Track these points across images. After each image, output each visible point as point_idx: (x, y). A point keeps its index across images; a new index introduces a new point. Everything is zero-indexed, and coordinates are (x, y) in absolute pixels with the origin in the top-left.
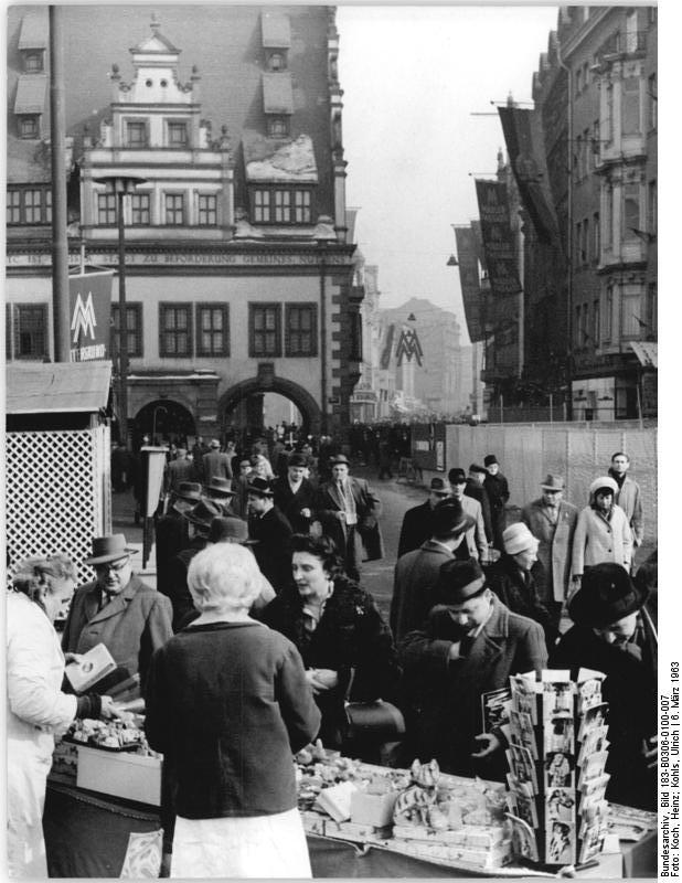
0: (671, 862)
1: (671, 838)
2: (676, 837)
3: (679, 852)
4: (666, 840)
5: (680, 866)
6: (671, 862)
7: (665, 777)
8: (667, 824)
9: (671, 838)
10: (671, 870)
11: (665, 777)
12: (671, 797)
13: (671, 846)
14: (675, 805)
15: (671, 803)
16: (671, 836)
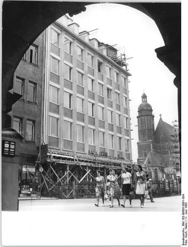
1: (185, 235)
2: (186, 234)
3: (187, 238)
4: (184, 235)
5: (187, 242)
8: (184, 230)
9: (185, 235)
11: (183, 217)
14: (186, 225)
15: (185, 225)
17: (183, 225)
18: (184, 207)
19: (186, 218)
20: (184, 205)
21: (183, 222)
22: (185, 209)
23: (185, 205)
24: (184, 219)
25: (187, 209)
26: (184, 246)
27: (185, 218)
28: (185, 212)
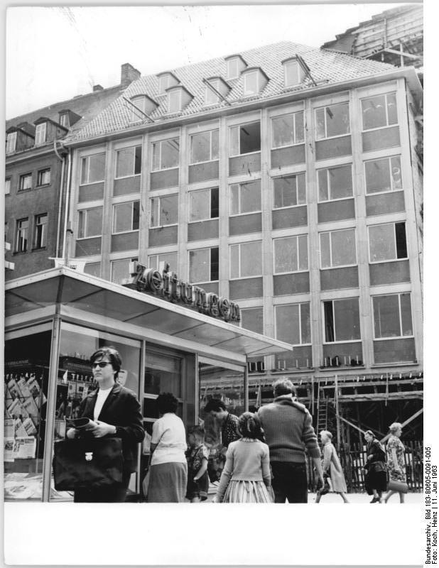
0: (432, 554)
1: (432, 541)
2: (435, 539)
3: (437, 548)
4: (429, 540)
5: (438, 557)
6: (432, 554)
7: (428, 500)
8: (429, 530)
9: (432, 539)
10: (432, 559)
11: (428, 500)
12: (432, 513)
13: (432, 544)
14: (435, 518)
15: (432, 517)
16: (432, 538)
17: (428, 518)
18: (431, 475)
19: (434, 501)
20: (431, 470)
21: (429, 511)
22: (432, 480)
23: (432, 472)
24: (431, 504)
25: (437, 480)
26: (431, 565)
27: (432, 501)
28: (432, 488)
